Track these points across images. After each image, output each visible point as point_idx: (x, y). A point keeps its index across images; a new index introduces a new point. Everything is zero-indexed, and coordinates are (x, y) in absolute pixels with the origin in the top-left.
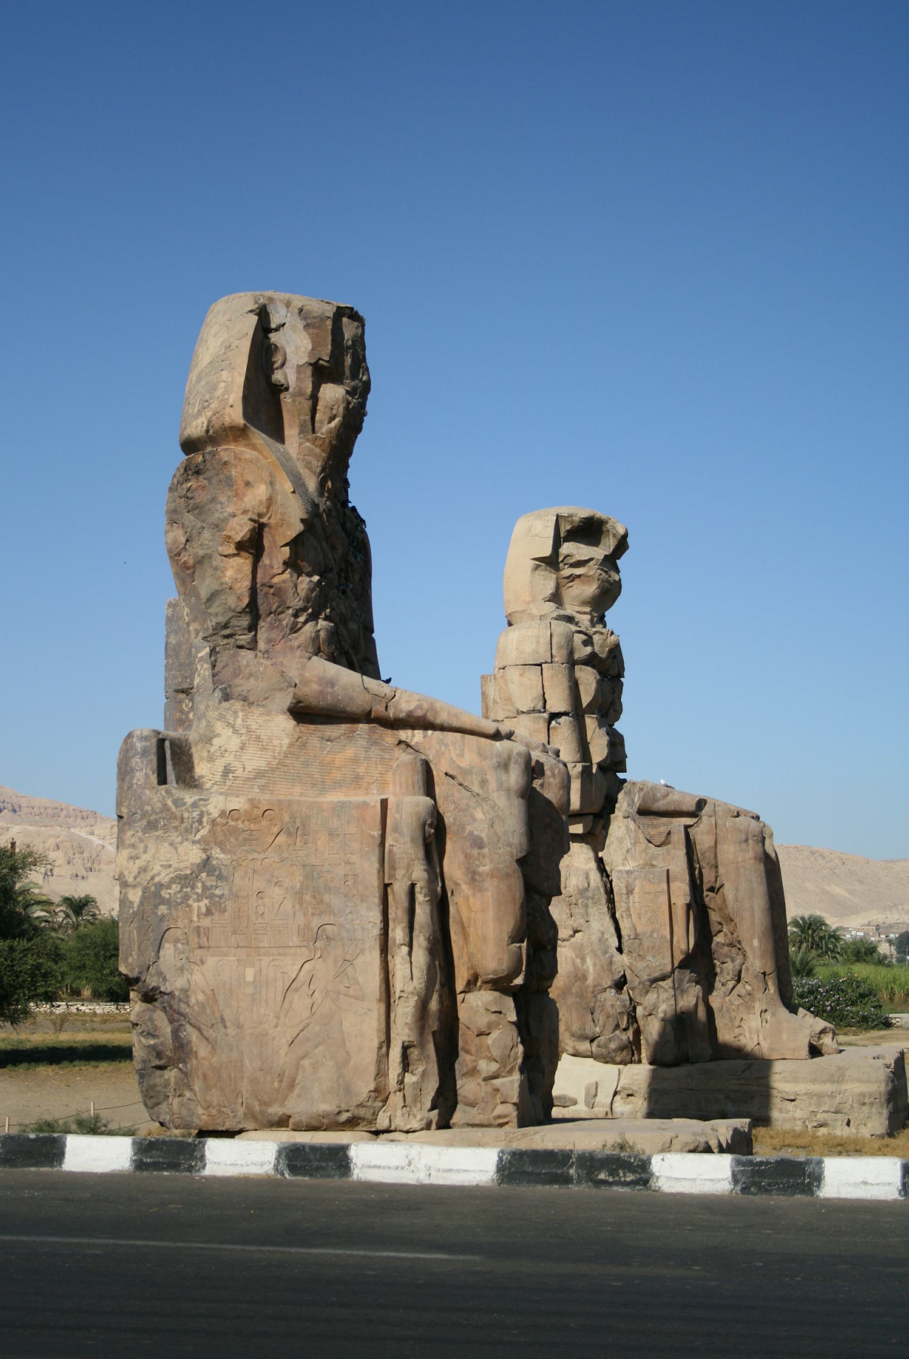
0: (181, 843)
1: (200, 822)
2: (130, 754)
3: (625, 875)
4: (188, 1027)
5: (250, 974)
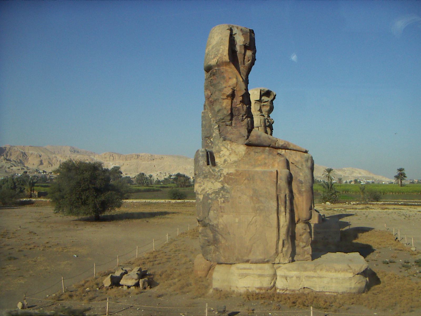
0: (215, 182)
1: (221, 176)
4: (219, 235)
5: (237, 220)
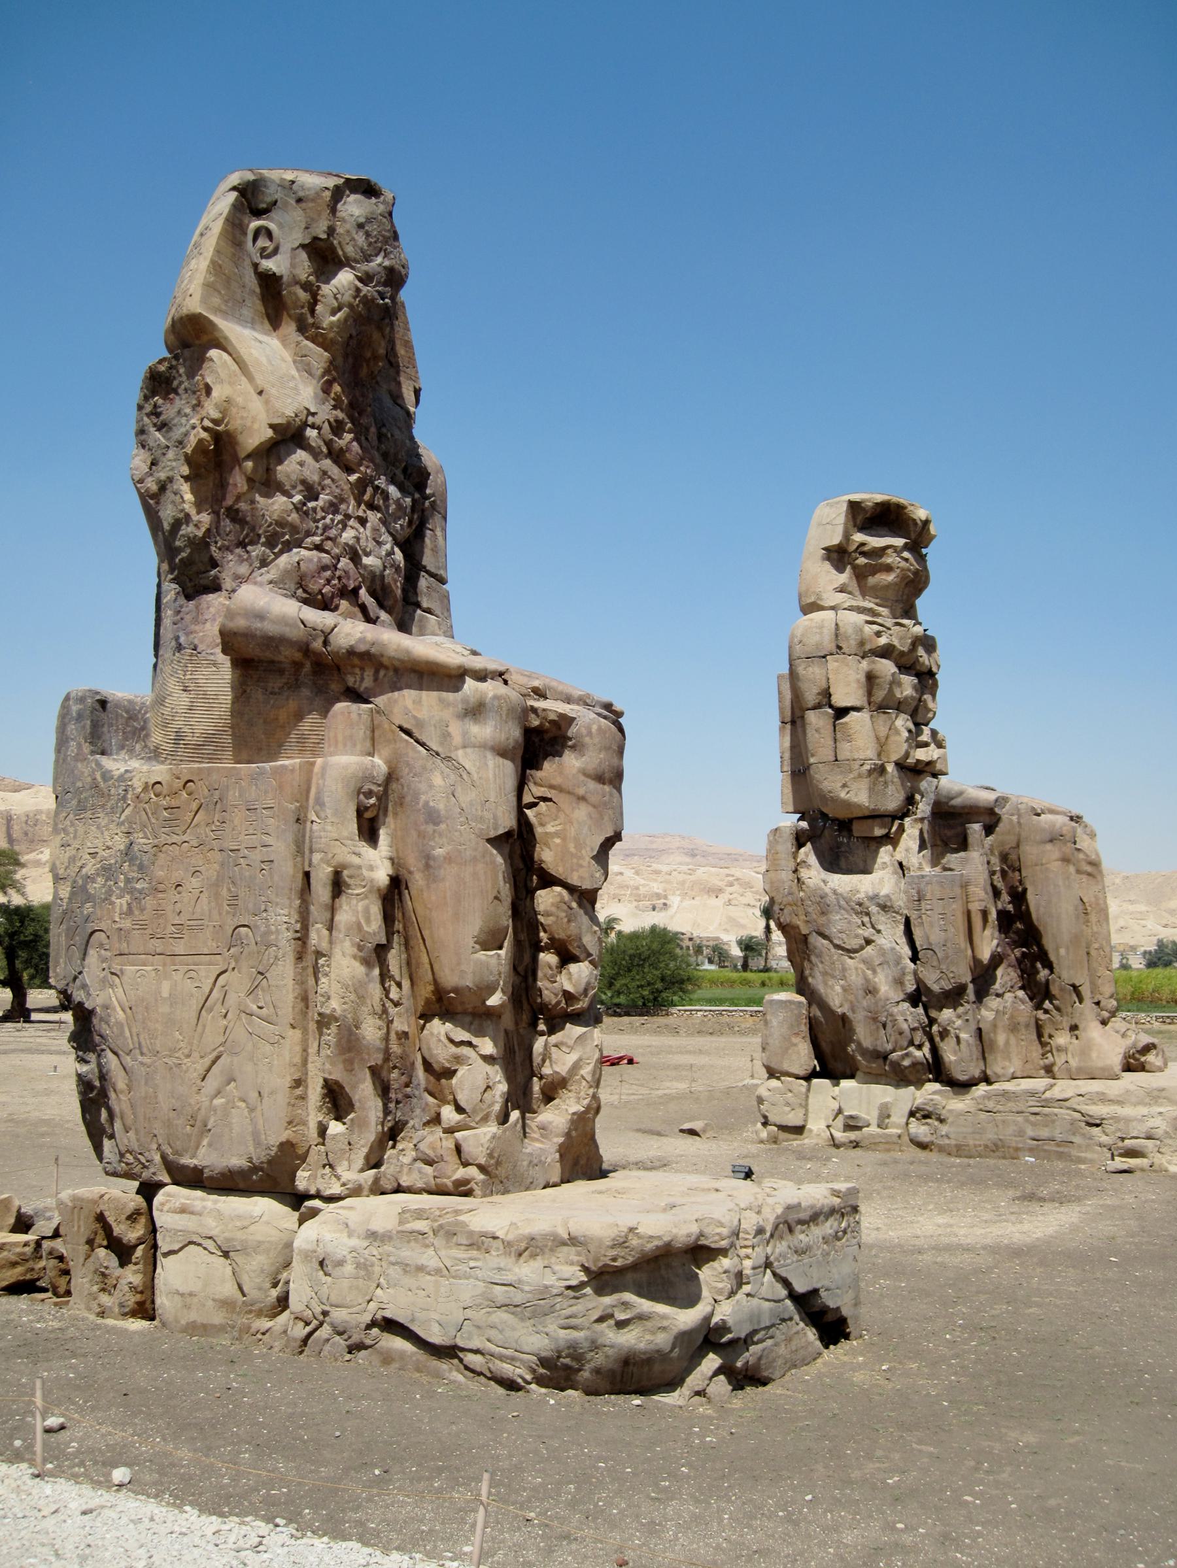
1: (124, 798)
2: (67, 720)
3: (916, 881)
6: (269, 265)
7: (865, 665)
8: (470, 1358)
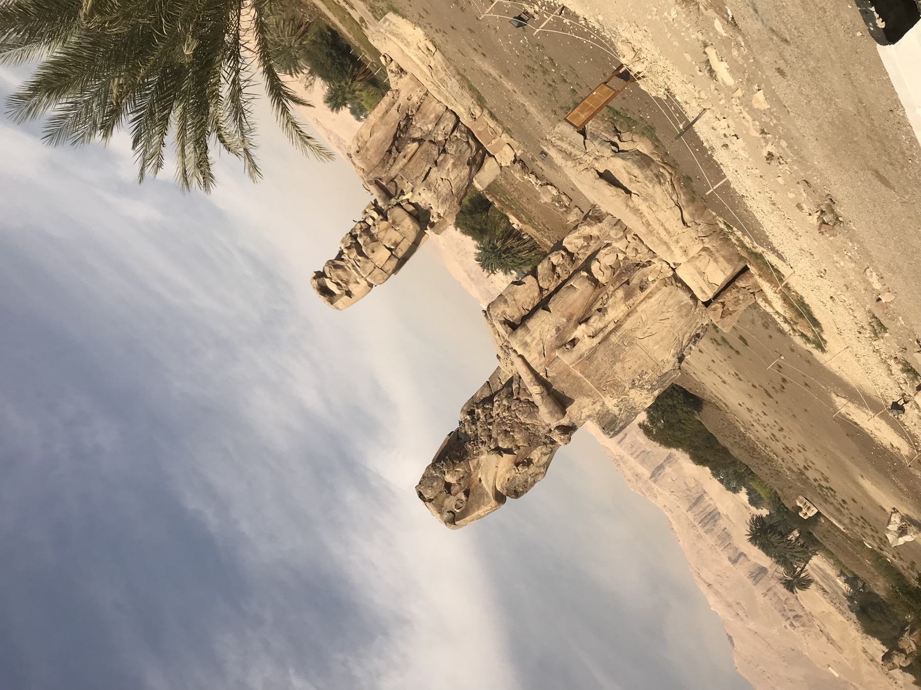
6: (463, 498)
7: (371, 256)
8: (675, 199)
